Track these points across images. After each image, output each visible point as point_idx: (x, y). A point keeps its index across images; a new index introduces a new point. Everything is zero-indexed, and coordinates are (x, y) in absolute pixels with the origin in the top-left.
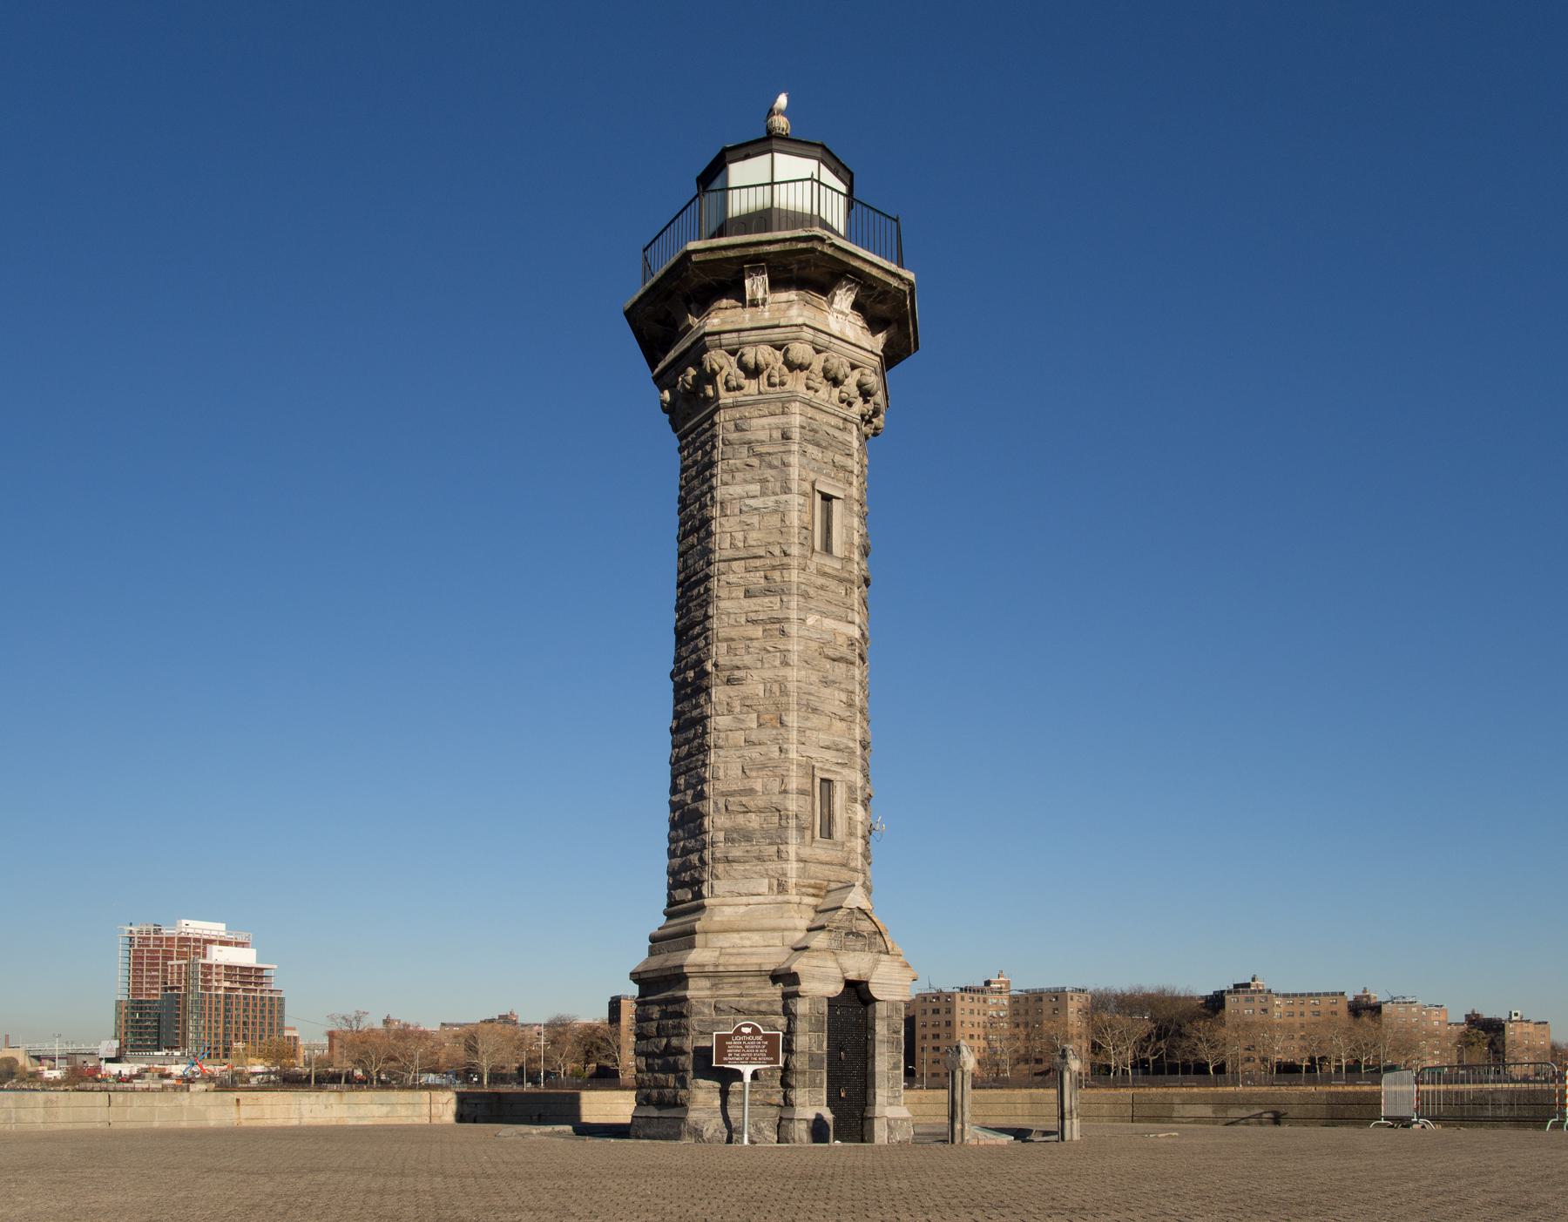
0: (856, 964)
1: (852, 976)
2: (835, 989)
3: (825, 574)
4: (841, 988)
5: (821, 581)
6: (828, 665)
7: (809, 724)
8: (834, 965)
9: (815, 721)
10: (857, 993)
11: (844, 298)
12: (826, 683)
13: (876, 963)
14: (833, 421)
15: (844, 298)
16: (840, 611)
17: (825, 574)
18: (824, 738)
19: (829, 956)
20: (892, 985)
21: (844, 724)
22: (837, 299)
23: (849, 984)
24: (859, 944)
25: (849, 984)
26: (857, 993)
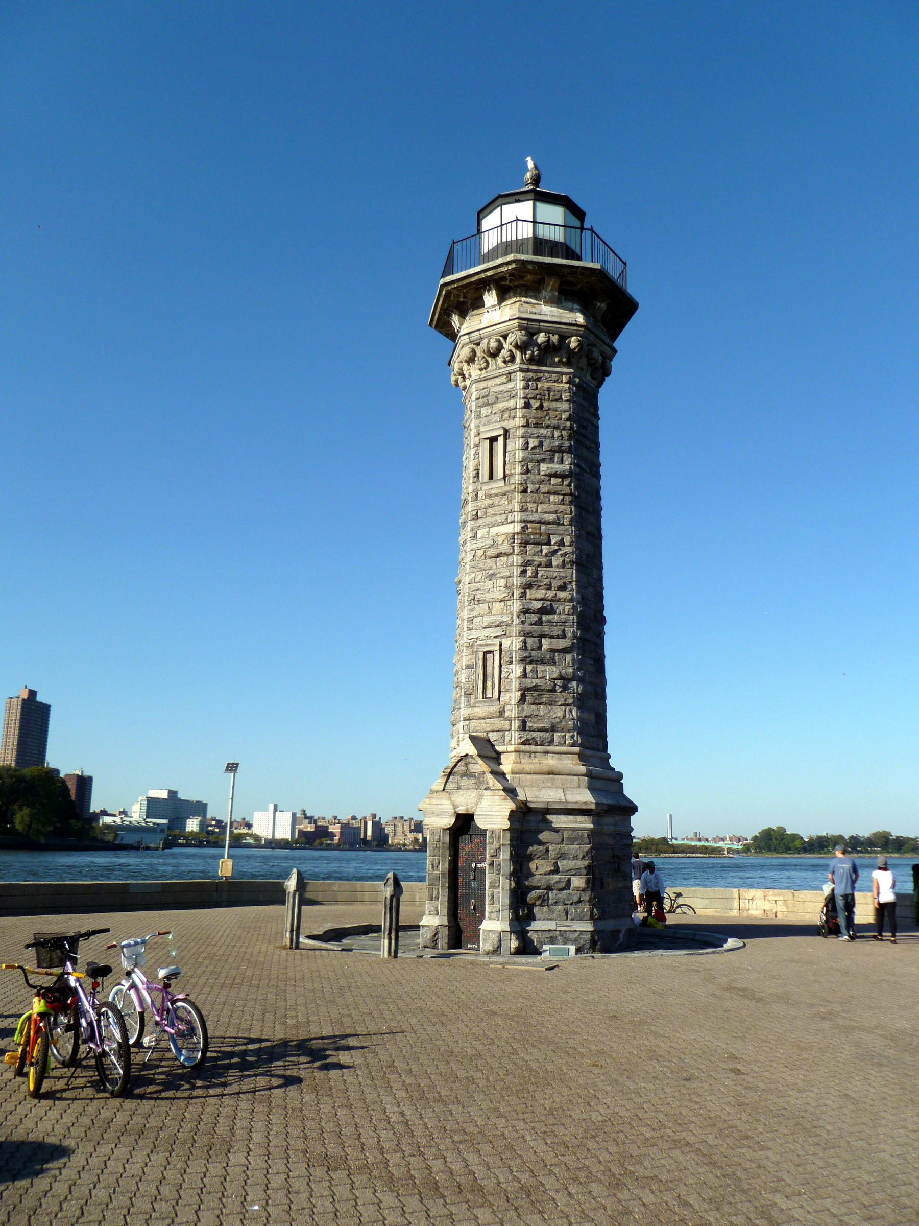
0: (464, 801)
1: (462, 810)
2: (450, 821)
3: (490, 496)
5: (488, 501)
7: (474, 614)
8: (448, 802)
9: (479, 609)
12: (491, 577)
13: (480, 797)
14: (498, 381)
15: (490, 298)
17: (490, 496)
18: (486, 620)
19: (444, 794)
21: (502, 604)
22: (486, 301)
23: (459, 816)
24: (472, 781)
25: (459, 816)
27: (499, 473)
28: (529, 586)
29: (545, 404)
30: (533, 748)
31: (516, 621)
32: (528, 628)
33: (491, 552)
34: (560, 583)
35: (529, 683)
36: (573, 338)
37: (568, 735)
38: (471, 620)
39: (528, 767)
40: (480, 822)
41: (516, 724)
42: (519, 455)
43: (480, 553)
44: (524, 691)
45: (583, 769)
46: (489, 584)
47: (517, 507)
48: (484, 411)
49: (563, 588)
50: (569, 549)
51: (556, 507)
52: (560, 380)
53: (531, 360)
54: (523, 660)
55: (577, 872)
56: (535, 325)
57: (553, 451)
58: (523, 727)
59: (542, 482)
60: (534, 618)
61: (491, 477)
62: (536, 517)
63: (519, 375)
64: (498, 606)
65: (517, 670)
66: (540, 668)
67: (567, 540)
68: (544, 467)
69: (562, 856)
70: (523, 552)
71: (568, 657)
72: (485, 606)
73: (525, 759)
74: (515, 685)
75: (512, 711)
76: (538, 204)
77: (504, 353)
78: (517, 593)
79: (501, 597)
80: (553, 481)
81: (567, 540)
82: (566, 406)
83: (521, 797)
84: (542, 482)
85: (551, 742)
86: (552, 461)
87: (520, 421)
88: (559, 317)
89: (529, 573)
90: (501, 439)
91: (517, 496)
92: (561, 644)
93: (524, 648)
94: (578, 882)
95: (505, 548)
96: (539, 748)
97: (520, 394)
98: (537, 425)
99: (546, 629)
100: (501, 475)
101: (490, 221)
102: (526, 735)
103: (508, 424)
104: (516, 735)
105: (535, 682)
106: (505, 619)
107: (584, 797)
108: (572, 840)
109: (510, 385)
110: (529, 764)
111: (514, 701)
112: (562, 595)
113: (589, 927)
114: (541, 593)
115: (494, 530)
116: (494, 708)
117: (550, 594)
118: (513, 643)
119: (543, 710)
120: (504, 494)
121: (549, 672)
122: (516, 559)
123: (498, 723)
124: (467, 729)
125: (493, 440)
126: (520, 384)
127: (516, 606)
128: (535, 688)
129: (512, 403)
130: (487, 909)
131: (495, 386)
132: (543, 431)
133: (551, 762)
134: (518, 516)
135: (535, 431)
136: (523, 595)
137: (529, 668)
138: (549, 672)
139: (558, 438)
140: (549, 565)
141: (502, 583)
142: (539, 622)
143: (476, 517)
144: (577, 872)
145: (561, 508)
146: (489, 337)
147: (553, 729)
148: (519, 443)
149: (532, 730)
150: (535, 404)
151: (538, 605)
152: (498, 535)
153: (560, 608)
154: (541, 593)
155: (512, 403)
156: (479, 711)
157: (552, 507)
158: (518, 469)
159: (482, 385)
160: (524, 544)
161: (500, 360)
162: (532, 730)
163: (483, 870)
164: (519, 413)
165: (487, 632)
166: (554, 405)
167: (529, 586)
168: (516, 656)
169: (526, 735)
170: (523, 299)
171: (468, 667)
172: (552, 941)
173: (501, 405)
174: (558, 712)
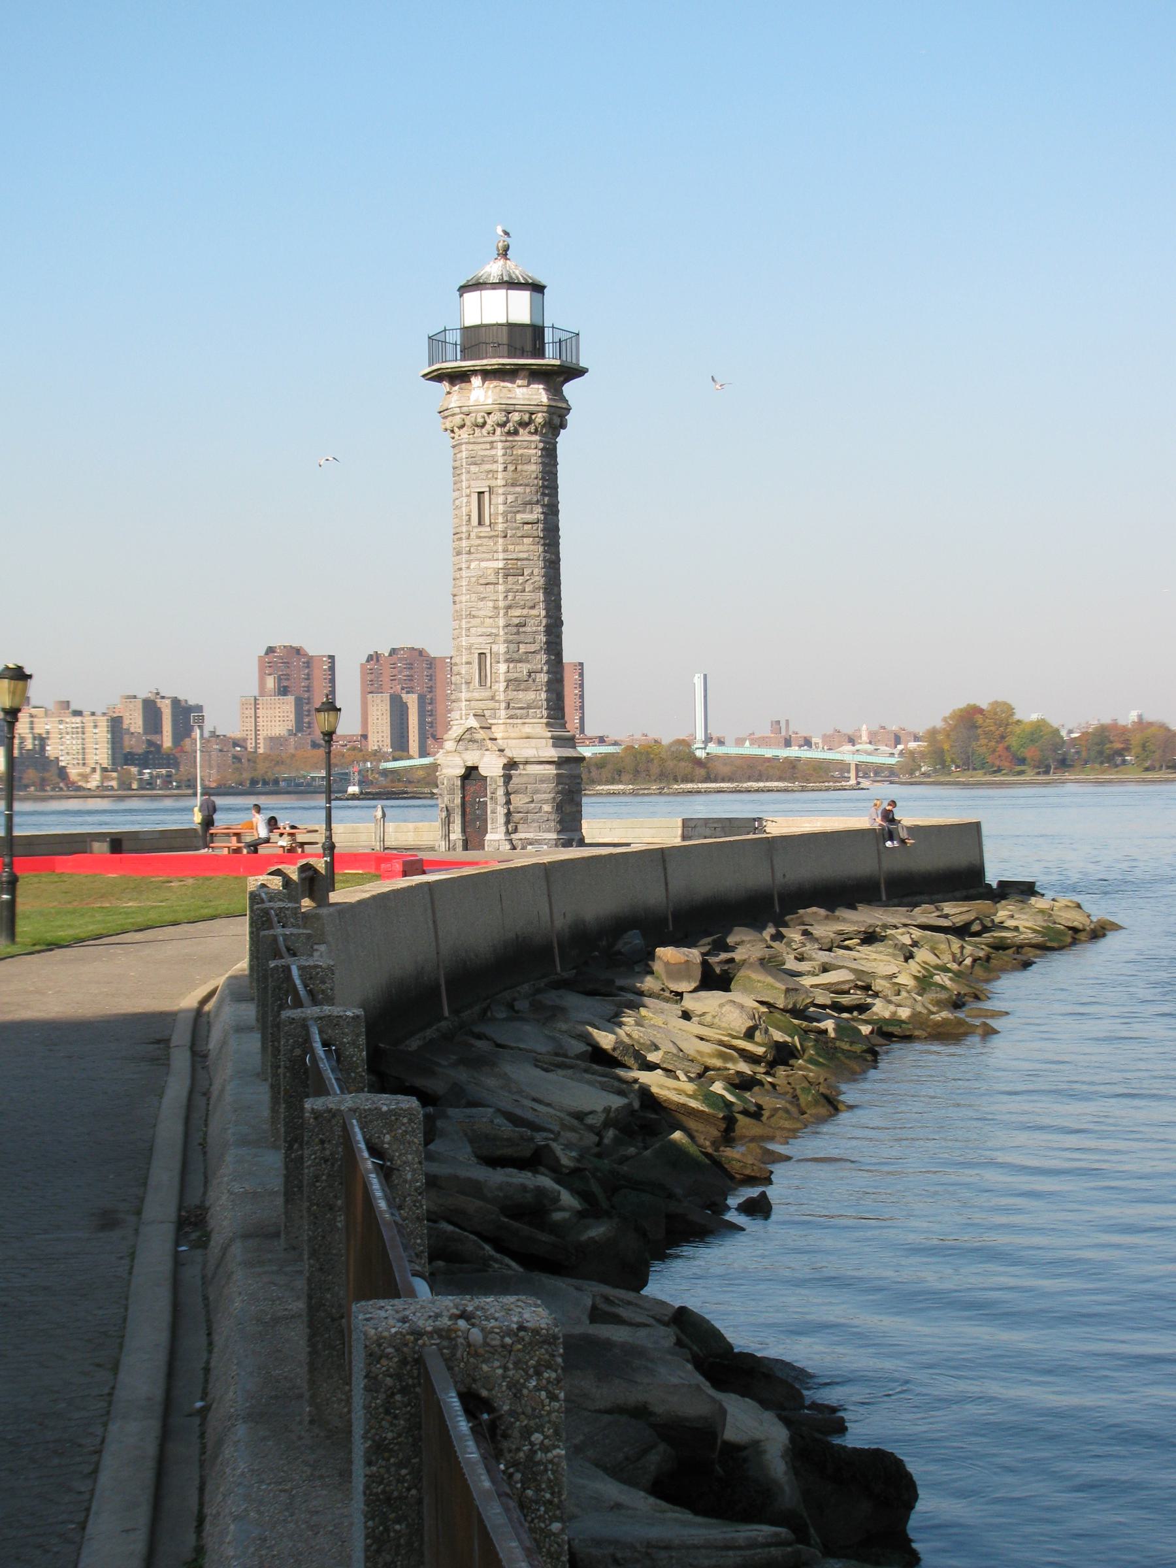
0: (471, 758)
1: (470, 764)
3: (480, 537)
4: (463, 771)
5: (479, 542)
6: (481, 588)
10: (471, 772)
11: (476, 381)
12: (482, 599)
14: (484, 446)
15: (476, 381)
16: (489, 556)
17: (480, 537)
18: (481, 630)
20: (491, 766)
24: (475, 746)
26: (471, 772)
27: (487, 522)
28: (509, 607)
29: (519, 467)
30: (515, 721)
31: (502, 633)
32: (511, 637)
33: (483, 581)
34: (531, 604)
35: (512, 676)
36: (540, 415)
37: (538, 711)
38: (468, 629)
39: (513, 735)
40: (483, 771)
41: (503, 705)
42: (501, 508)
43: (473, 579)
44: (508, 681)
45: (549, 734)
46: (481, 604)
47: (500, 549)
48: (474, 469)
49: (533, 607)
50: (537, 578)
51: (530, 550)
52: (529, 444)
53: (509, 433)
54: (507, 661)
55: (546, 802)
56: (512, 408)
57: (525, 504)
58: (508, 707)
59: (518, 528)
60: (515, 630)
61: (480, 524)
62: (514, 556)
63: (500, 445)
64: (488, 620)
65: (503, 667)
66: (519, 665)
67: (536, 571)
68: (519, 516)
69: (536, 792)
70: (505, 582)
71: (538, 657)
72: (478, 620)
73: (510, 729)
74: (502, 678)
75: (501, 696)
76: (510, 292)
77: (488, 427)
78: (502, 612)
79: (490, 614)
80: (526, 527)
81: (536, 571)
82: (533, 467)
83: (508, 753)
84: (518, 528)
85: (527, 716)
86: (524, 512)
87: (500, 482)
88: (529, 399)
89: (510, 598)
90: (487, 495)
91: (501, 540)
92: (532, 648)
93: (507, 652)
94: (547, 808)
95: (492, 579)
96: (519, 721)
97: (501, 460)
98: (513, 485)
99: (522, 638)
100: (487, 523)
101: (471, 297)
102: (511, 712)
103: (493, 483)
104: (503, 713)
105: (516, 675)
106: (494, 631)
107: (552, 753)
108: (542, 781)
109: (493, 452)
110: (514, 733)
111: (502, 689)
112: (534, 612)
113: (554, 836)
114: (518, 612)
115: (484, 564)
116: (488, 694)
117: (525, 612)
118: (501, 648)
119: (521, 695)
120: (490, 537)
121: (524, 668)
122: (501, 588)
123: (491, 704)
124: (469, 708)
125: (479, 493)
126: (500, 452)
127: (501, 622)
128: (516, 680)
129: (494, 467)
130: (489, 826)
131: (481, 451)
132: (518, 489)
133: (527, 730)
134: (501, 556)
135: (511, 489)
136: (506, 614)
137: (512, 665)
138: (524, 668)
139: (528, 492)
140: (524, 591)
141: (491, 604)
142: (518, 633)
143: (469, 553)
144: (546, 802)
145: (532, 547)
146: (477, 412)
147: (529, 708)
148: (501, 499)
149: (514, 708)
150: (511, 468)
151: (516, 621)
152: (487, 568)
153: (531, 622)
154: (518, 612)
155: (494, 467)
156: (476, 695)
157: (525, 548)
158: (500, 520)
159: (471, 447)
160: (506, 576)
161: (484, 431)
162: (514, 708)
163: (485, 803)
164: (500, 475)
165: (481, 639)
166: (526, 467)
167: (509, 607)
168: (502, 658)
169: (511, 712)
170: (502, 384)
171: (468, 663)
172: (531, 844)
173: (488, 467)
174: (531, 696)
